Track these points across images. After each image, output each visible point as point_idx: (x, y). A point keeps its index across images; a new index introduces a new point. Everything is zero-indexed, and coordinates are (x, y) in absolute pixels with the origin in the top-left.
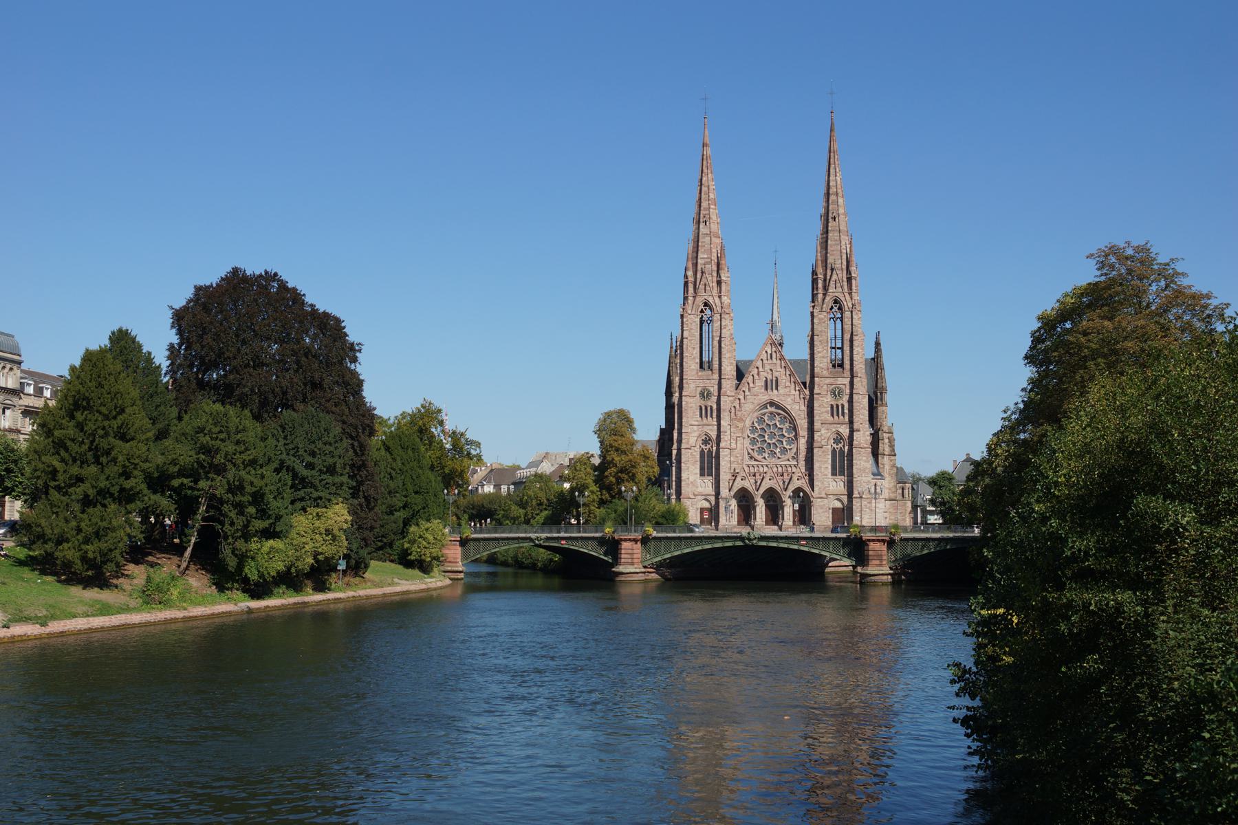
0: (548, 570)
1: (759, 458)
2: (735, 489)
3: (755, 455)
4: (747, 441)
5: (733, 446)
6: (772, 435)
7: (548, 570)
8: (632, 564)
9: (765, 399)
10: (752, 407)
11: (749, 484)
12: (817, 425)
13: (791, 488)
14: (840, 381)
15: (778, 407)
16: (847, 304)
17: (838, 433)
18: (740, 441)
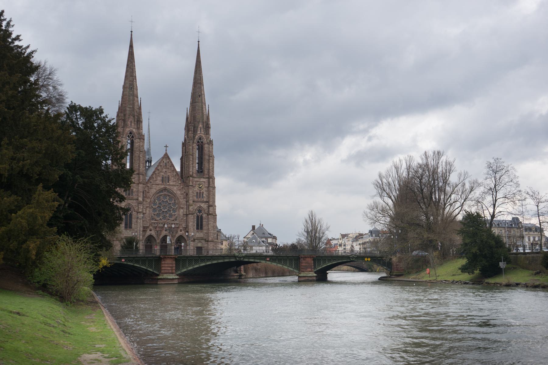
0: (517, 262)
1: (158, 219)
2: (146, 236)
3: (156, 217)
4: (151, 210)
5: (144, 212)
6: (165, 207)
7: (517, 262)
8: (172, 273)
9: (163, 186)
10: (155, 191)
11: (153, 233)
12: (191, 202)
13: (177, 236)
14: (202, 180)
15: (168, 191)
16: (205, 141)
17: (200, 207)
18: (148, 209)
